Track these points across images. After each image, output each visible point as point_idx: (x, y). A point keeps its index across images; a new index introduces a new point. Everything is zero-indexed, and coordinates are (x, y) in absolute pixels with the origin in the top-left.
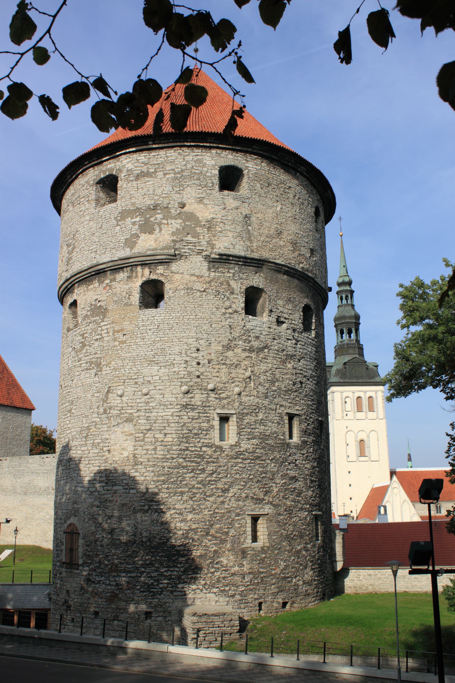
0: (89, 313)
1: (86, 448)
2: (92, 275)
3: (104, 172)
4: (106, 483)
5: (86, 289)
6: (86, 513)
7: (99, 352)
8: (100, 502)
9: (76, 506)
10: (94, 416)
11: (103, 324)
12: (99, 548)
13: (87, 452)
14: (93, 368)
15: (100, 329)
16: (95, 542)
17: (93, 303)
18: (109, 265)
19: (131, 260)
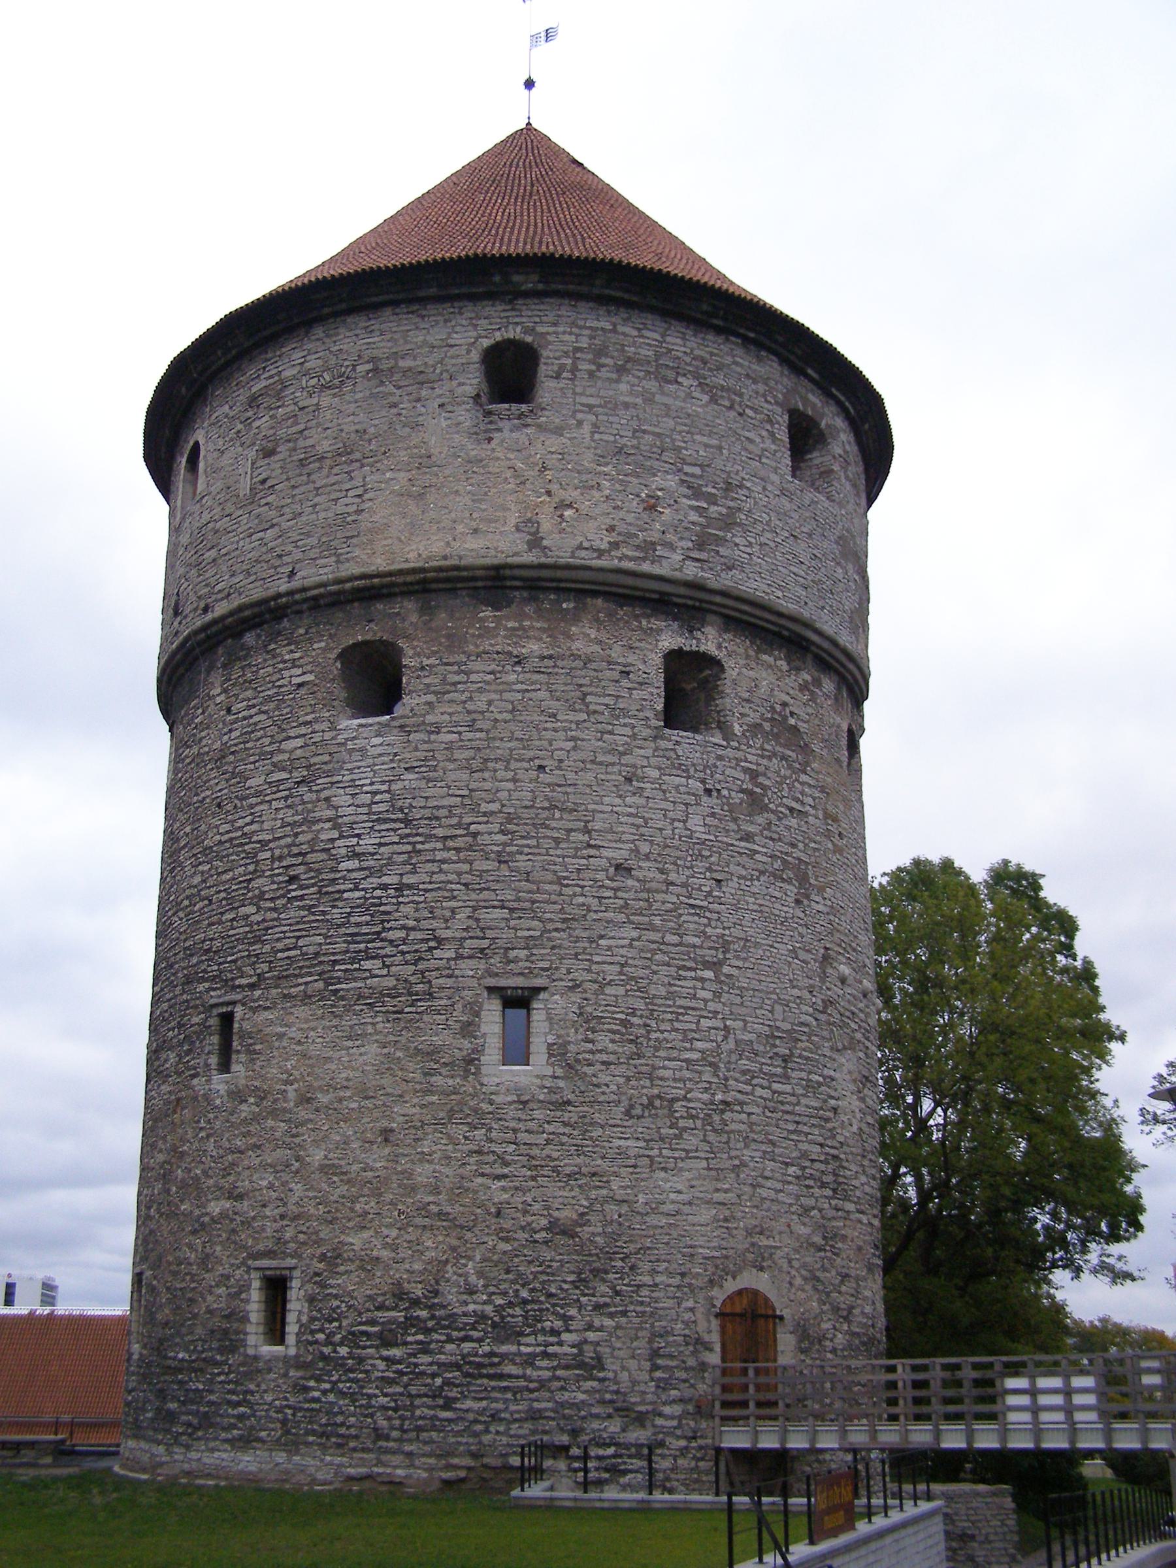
0: (767, 726)
1: (788, 1088)
2: (778, 635)
3: (805, 401)
4: (834, 1191)
5: (751, 653)
6: (796, 1264)
7: (801, 845)
8: (825, 1238)
9: (764, 1242)
10: (804, 1008)
11: (803, 778)
12: (829, 1356)
13: (793, 1099)
14: (789, 881)
15: (796, 784)
16: (820, 1341)
17: (778, 708)
18: (826, 645)
19: (851, 666)
